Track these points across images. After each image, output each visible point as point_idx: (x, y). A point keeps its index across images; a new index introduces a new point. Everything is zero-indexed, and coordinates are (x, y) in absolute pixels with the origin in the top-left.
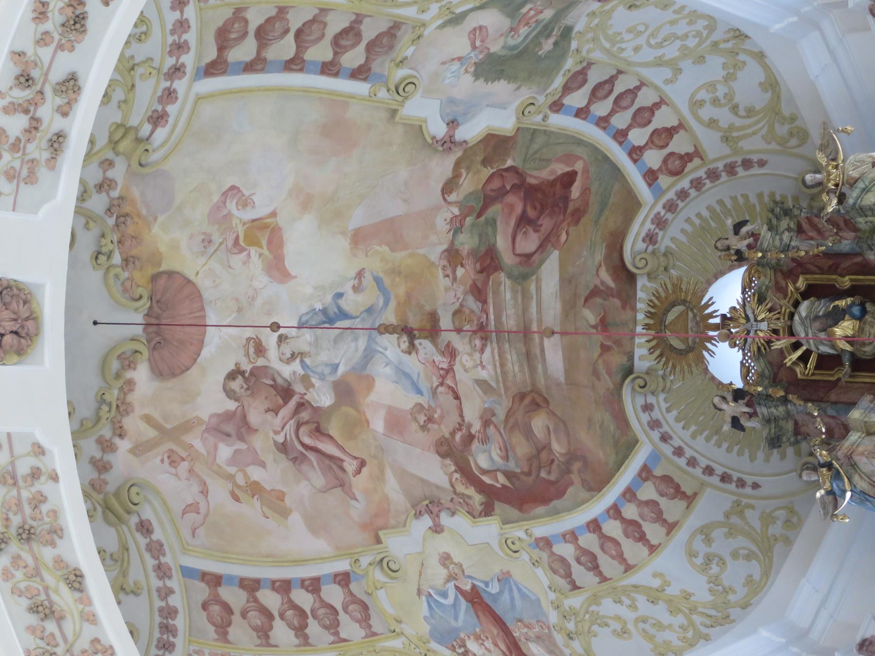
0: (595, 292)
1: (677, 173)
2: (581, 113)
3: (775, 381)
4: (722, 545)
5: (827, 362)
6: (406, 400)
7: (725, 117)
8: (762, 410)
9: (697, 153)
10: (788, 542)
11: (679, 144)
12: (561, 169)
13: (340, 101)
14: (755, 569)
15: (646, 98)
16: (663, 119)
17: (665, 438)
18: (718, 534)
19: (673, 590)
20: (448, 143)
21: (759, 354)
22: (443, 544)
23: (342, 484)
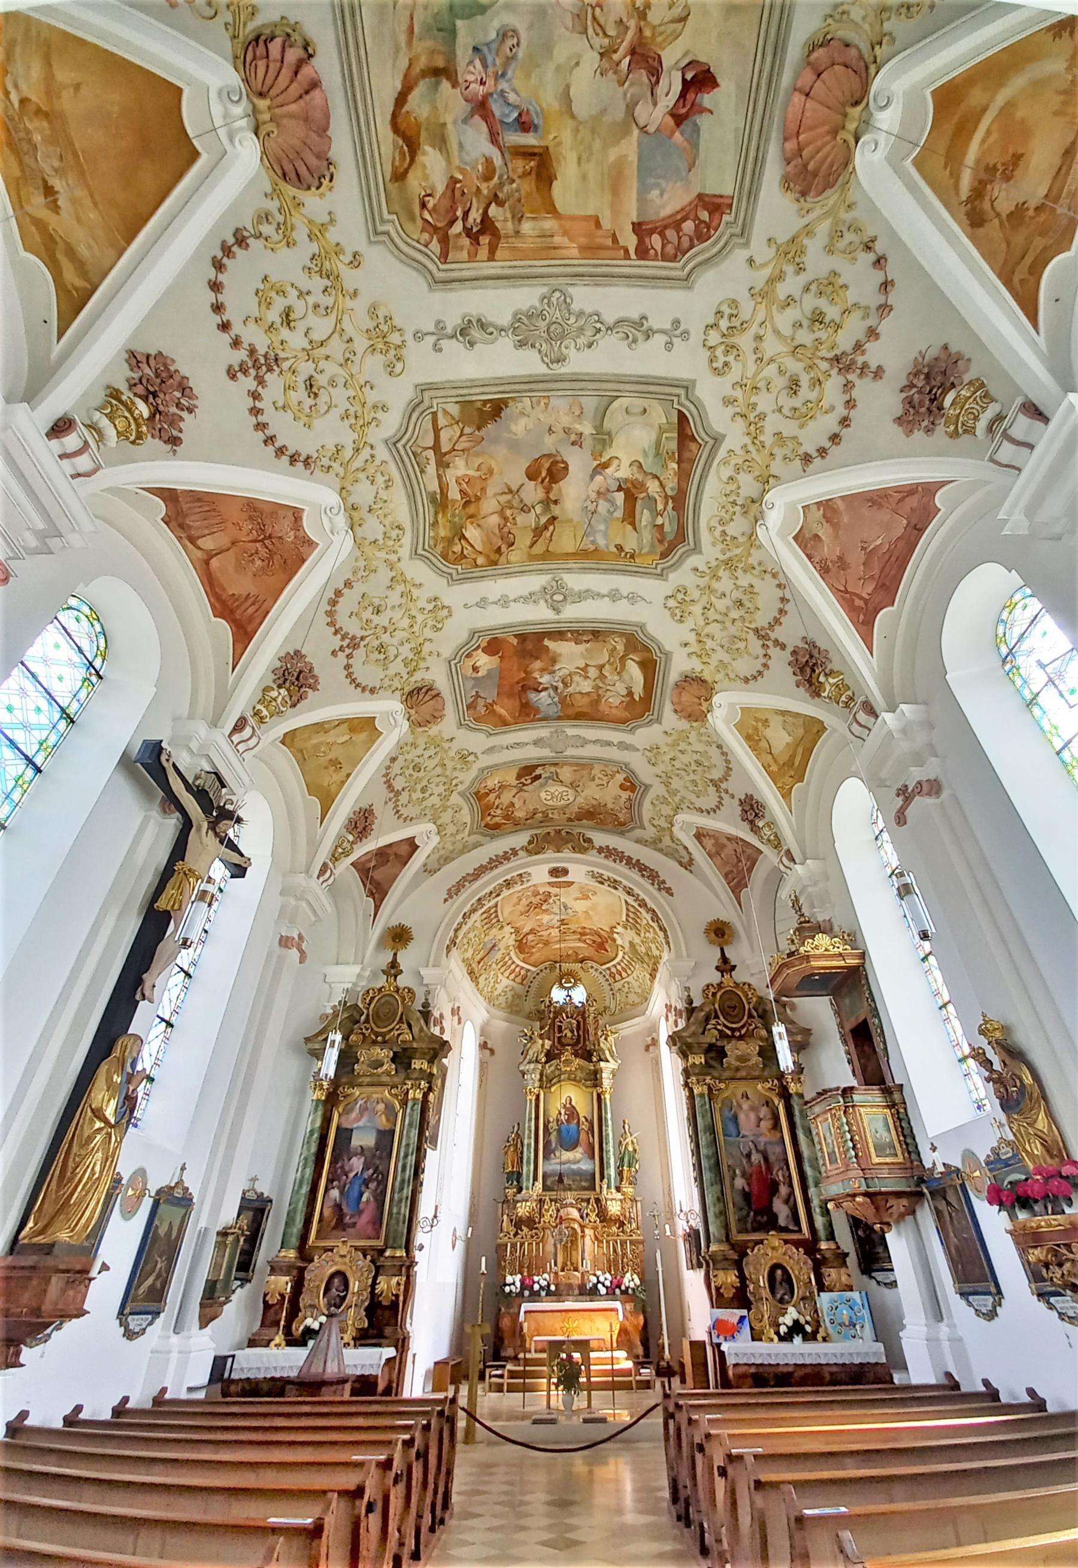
4: (509, 995)
5: (560, 1031)
6: (545, 921)
7: (626, 990)
10: (511, 1013)
11: (618, 977)
13: (621, 916)
14: (503, 1005)
15: (629, 972)
16: (624, 975)
20: (613, 932)
21: (561, 1007)
22: (507, 935)
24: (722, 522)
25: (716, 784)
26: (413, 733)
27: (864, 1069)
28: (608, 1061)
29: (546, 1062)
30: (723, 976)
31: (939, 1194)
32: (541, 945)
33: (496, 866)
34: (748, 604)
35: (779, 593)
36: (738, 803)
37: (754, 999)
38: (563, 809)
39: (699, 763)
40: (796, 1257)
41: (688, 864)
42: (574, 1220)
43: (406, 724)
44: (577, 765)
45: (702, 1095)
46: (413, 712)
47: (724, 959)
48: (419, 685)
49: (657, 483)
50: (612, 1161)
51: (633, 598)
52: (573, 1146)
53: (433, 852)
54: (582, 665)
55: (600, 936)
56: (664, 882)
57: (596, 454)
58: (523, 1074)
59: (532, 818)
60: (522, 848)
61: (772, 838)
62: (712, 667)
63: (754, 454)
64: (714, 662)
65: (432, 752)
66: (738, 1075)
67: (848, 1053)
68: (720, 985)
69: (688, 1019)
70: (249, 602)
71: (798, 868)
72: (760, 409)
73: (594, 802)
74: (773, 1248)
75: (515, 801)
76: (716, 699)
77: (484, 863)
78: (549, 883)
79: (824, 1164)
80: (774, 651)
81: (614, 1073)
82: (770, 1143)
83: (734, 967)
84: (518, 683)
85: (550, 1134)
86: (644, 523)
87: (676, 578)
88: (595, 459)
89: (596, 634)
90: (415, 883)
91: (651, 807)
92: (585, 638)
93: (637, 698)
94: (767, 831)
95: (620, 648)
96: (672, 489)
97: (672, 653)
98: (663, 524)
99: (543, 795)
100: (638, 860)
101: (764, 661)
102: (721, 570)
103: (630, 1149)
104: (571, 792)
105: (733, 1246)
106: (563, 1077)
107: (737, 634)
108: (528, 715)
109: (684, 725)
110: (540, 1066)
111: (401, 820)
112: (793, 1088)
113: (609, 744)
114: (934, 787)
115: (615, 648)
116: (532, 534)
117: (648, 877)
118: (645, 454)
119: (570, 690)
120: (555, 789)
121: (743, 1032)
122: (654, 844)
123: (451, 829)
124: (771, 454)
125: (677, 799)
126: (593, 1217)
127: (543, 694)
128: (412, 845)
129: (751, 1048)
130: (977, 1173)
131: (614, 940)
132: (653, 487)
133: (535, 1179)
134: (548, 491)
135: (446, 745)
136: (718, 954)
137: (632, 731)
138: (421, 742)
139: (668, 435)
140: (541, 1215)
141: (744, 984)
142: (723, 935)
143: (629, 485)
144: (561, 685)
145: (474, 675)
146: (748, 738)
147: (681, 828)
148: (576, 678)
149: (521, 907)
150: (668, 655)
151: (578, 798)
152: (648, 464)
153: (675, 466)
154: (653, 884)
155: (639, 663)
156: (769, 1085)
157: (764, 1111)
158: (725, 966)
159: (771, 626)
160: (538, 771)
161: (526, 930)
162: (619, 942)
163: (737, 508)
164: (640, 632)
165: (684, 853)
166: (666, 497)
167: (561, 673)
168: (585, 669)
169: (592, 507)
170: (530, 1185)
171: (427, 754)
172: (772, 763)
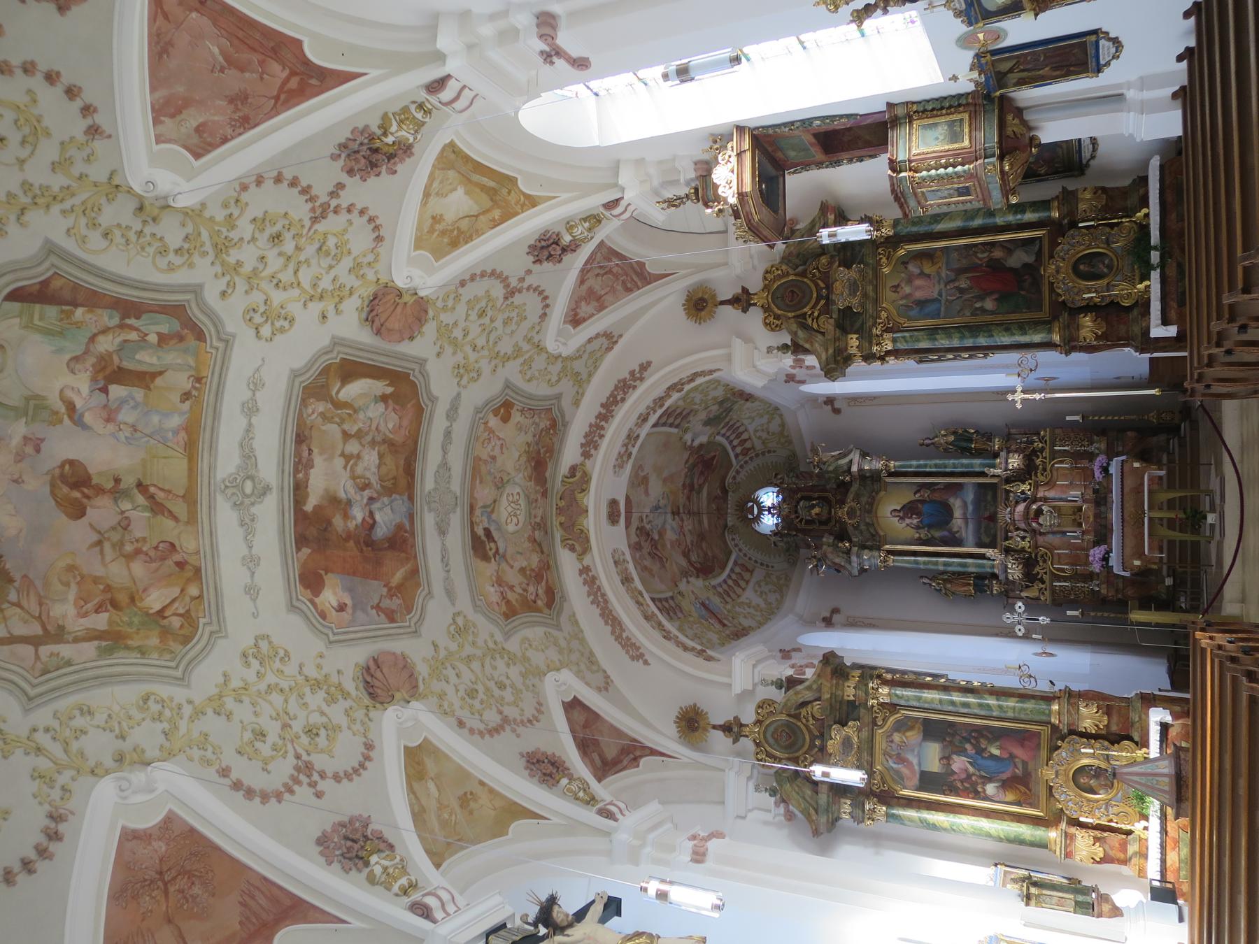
0: (716, 497)
1: (745, 455)
2: (723, 435)
3: (789, 529)
7: (764, 435)
8: (785, 539)
9: (753, 448)
11: (748, 445)
12: (713, 454)
16: (745, 436)
17: (740, 550)
18: (763, 584)
19: (754, 603)
20: (691, 447)
23: (663, 566)
24: (163, 251)
25: (511, 293)
26: (425, 697)
27: (868, 144)
28: (851, 461)
29: (850, 541)
30: (755, 304)
31: (1001, 79)
32: (704, 545)
33: (603, 595)
34: (278, 227)
35: (269, 184)
36: (537, 266)
37: (784, 267)
38: (531, 502)
39: (482, 314)
40: (1066, 247)
41: (610, 339)
42: (1027, 508)
43: (414, 704)
44: (473, 478)
45: (894, 340)
46: (398, 695)
47: (734, 301)
48: (361, 686)
49: (101, 338)
50: (965, 461)
51: (256, 384)
52: (949, 511)
53: (583, 678)
54: (341, 461)
55: (694, 466)
56: (632, 373)
57: (55, 419)
58: (862, 571)
59: (540, 545)
60: (580, 560)
61: (587, 225)
62: (357, 283)
63: (77, 201)
64: (350, 281)
65: (451, 673)
66: (872, 294)
67: (850, 161)
68: (766, 309)
69: (807, 351)
70: (252, 903)
71: (629, 196)
72: (16, 189)
73: (524, 458)
74: (1058, 272)
75: (517, 565)
76: (401, 282)
77: (598, 611)
78: (627, 527)
79: (970, 202)
80: (345, 199)
81: (864, 455)
82: (947, 264)
83: (745, 291)
84: (362, 551)
85: (933, 537)
86: (154, 360)
87: (233, 321)
88: (61, 421)
89: (300, 439)
90: (624, 705)
91: (534, 382)
92: (305, 454)
93: (390, 390)
94: (578, 231)
95: (321, 407)
96: (111, 317)
97: (333, 337)
98: (159, 334)
99: (511, 528)
100: (602, 405)
101: (356, 212)
102: (227, 259)
103: (952, 438)
104: (508, 489)
105: (1055, 317)
106: (868, 520)
107: (317, 245)
108: (405, 541)
109: (430, 329)
110: (855, 549)
111: (541, 717)
112: (887, 231)
113: (448, 433)
114: (547, 23)
115: (322, 415)
116: (160, 517)
117: (625, 393)
118: (60, 351)
119: (374, 480)
120: (504, 509)
121: (822, 285)
122: (581, 382)
123: (553, 654)
124: (80, 178)
125: (526, 347)
126: (1025, 487)
127: (378, 517)
128: (573, 706)
129: (843, 275)
130: (981, 36)
131: (701, 446)
132: (106, 344)
133: (982, 557)
134: (100, 490)
135: (443, 653)
136: (728, 308)
137: (434, 400)
138: (437, 686)
139: (36, 316)
140: (1023, 550)
141: (765, 278)
142: (702, 300)
143: (101, 376)
144: (367, 493)
145: (349, 610)
146: (454, 244)
147: (565, 344)
148: (359, 470)
149: (656, 568)
150: (336, 342)
151: (517, 480)
152: (75, 347)
153: (80, 311)
154: (635, 387)
155: (343, 385)
156: (884, 260)
157: (913, 268)
158: (742, 301)
159: (312, 199)
160: (480, 532)
161: (683, 562)
162: (703, 439)
163: (147, 230)
164: (301, 379)
165: (596, 345)
166: (122, 326)
167: (351, 491)
168: (347, 458)
169: (127, 432)
170: (990, 562)
171: (453, 679)
172: (490, 216)
